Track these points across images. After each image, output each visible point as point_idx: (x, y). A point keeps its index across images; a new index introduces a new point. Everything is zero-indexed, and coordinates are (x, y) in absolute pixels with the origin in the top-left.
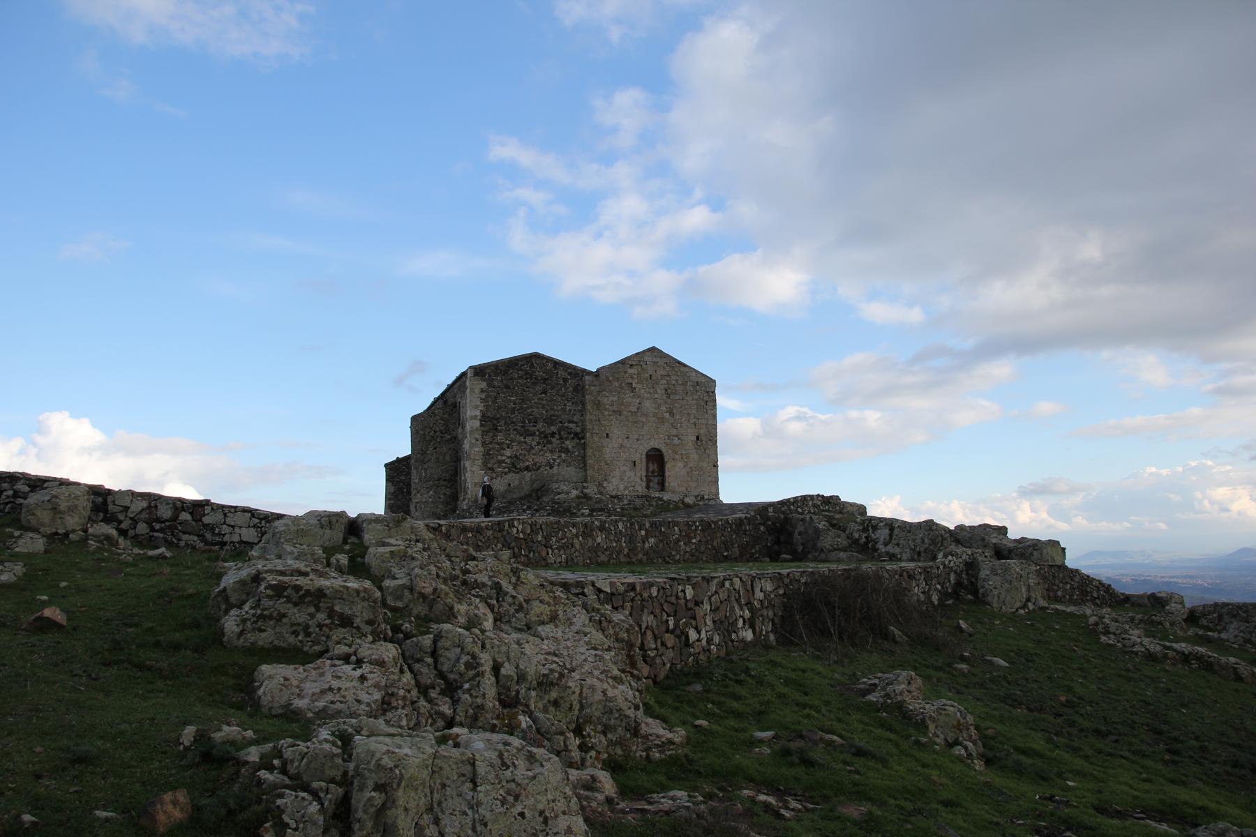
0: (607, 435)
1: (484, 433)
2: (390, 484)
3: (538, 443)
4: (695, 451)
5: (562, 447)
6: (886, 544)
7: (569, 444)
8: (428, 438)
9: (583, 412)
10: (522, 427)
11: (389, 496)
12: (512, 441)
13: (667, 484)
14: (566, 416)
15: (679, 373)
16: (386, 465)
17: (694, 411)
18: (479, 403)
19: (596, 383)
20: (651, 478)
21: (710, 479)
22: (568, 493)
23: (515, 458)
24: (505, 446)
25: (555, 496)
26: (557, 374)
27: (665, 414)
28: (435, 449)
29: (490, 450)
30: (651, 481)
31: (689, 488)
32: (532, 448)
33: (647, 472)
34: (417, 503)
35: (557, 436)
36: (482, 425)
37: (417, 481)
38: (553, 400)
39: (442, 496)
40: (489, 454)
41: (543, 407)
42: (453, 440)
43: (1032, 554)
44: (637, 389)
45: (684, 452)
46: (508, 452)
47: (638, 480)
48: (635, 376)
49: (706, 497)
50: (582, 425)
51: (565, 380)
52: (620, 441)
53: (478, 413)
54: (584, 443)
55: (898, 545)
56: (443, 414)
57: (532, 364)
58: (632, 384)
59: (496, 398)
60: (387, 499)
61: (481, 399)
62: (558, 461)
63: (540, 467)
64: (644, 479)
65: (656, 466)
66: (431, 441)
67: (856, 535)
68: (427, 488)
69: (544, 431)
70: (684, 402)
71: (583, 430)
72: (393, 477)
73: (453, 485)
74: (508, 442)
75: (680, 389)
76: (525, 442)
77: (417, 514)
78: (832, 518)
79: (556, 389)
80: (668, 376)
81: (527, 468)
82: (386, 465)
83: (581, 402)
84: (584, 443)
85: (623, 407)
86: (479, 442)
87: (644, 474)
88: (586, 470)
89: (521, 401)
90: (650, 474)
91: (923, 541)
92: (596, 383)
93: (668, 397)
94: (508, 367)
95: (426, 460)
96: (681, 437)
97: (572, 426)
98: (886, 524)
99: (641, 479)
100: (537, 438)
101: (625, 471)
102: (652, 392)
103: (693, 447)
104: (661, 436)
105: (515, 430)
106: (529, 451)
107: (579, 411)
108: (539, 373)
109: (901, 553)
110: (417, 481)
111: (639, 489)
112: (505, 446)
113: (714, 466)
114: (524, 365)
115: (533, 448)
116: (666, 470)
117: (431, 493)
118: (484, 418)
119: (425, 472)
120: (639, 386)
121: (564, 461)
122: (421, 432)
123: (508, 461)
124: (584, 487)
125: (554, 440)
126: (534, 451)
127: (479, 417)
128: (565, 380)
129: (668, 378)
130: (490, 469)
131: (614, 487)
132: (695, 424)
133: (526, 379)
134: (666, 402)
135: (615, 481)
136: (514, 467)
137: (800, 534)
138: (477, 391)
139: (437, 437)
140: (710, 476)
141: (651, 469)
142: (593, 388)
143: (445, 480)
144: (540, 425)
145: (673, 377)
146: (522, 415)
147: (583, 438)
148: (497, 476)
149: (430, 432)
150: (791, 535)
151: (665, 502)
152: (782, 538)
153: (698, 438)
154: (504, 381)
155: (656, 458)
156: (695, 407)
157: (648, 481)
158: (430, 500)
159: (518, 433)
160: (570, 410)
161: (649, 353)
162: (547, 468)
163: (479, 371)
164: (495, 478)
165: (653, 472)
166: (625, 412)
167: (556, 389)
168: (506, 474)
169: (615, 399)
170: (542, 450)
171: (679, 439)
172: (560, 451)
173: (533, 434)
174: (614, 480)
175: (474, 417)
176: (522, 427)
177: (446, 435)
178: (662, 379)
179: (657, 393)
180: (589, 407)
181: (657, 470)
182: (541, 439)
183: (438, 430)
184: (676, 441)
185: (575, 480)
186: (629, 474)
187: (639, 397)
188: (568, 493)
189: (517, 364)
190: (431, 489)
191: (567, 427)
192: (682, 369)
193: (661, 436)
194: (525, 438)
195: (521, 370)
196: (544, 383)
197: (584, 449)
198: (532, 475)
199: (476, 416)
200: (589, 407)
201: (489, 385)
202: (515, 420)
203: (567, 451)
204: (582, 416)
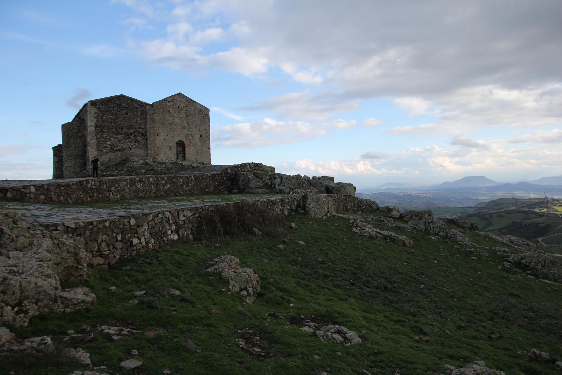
0: (158, 134)
1: (97, 134)
2: (55, 157)
3: (124, 138)
4: (199, 142)
5: (136, 140)
6: (279, 185)
7: (139, 138)
8: (70, 135)
9: (146, 123)
10: (116, 130)
11: (55, 163)
12: (111, 137)
13: (186, 157)
14: (138, 125)
15: (192, 105)
16: (53, 148)
18: (94, 119)
19: (152, 110)
20: (179, 154)
21: (207, 155)
22: (138, 162)
23: (113, 145)
24: (107, 140)
25: (132, 163)
26: (133, 105)
27: (185, 125)
28: (74, 141)
29: (100, 142)
30: (179, 156)
32: (121, 140)
33: (177, 151)
34: (66, 167)
35: (133, 135)
36: (95, 130)
37: (65, 156)
38: (131, 118)
39: (78, 164)
40: (99, 144)
41: (126, 121)
42: (83, 136)
43: (341, 190)
44: (172, 113)
45: (195, 142)
46: (109, 143)
47: (172, 155)
48: (171, 107)
49: (205, 163)
50: (146, 129)
51: (137, 108)
52: (164, 137)
53: (93, 124)
54: (147, 138)
55: (284, 186)
56: (77, 124)
57: (120, 100)
58: (169, 110)
59: (102, 116)
60: (54, 164)
61: (95, 117)
62: (134, 146)
63: (125, 150)
64: (176, 155)
65: (181, 148)
66: (71, 137)
67: (267, 181)
68: (71, 160)
69: (126, 133)
70: (195, 119)
71: (146, 132)
72: (57, 154)
73: (84, 158)
74: (109, 138)
75: (192, 113)
76: (118, 138)
77: (66, 172)
78: (257, 173)
79: (132, 112)
80: (187, 106)
81: (119, 150)
82: (53, 148)
83: (145, 119)
84: (147, 138)
85: (165, 121)
86: (94, 138)
87: (175, 153)
88: (147, 151)
89: (115, 118)
90: (178, 152)
91: (295, 184)
92: (152, 110)
93: (187, 117)
94: (108, 101)
95: (69, 146)
96: (193, 135)
97: (141, 130)
98: (280, 177)
99: (174, 155)
100: (123, 136)
101: (166, 151)
102: (179, 114)
104: (184, 135)
105: (112, 132)
106: (119, 142)
107: (144, 123)
108: (124, 105)
109: (285, 189)
110: (65, 156)
111: (173, 159)
112: (107, 140)
113: (209, 149)
114: (116, 101)
115: (121, 140)
116: (186, 151)
117: (73, 162)
118: (96, 126)
119: (69, 152)
120: (173, 111)
121: (137, 147)
122: (67, 133)
123: (109, 147)
124: (146, 159)
125: (131, 137)
126: (122, 142)
127: (94, 126)
128: (137, 108)
129: (187, 108)
130: (101, 151)
132: (199, 129)
133: (117, 107)
134: (186, 119)
135: (162, 156)
136: (112, 149)
137: (242, 181)
138: (93, 113)
139: (75, 135)
140: (206, 153)
141: (179, 150)
142: (150, 112)
143: (79, 156)
144: (125, 130)
145: (189, 107)
146: (116, 125)
147: (146, 136)
148: (104, 154)
149: (71, 133)
150: (238, 181)
151: (184, 166)
152: (234, 183)
153: (201, 136)
154: (107, 108)
155: (181, 145)
157: (178, 156)
158: (73, 165)
159: (114, 133)
160: (139, 122)
162: (129, 150)
163: (93, 103)
164: (103, 155)
165: (180, 151)
166: (166, 124)
167: (132, 112)
168: (108, 153)
169: (161, 117)
170: (126, 141)
171: (192, 136)
172: (135, 142)
173: (121, 134)
174: (161, 155)
175: (92, 126)
176: (116, 130)
177: (79, 134)
178: (184, 108)
179: (181, 115)
180: (148, 121)
181: (181, 151)
182: (125, 136)
183: (75, 131)
184: (190, 137)
185: (142, 155)
186: (169, 152)
187: (173, 116)
188: (138, 162)
189: (113, 100)
190: (72, 160)
191: (138, 131)
192: (194, 103)
193: (184, 135)
194: (117, 136)
195: (115, 103)
196: (126, 109)
197: (147, 141)
198: (121, 153)
199: (93, 125)
200: (149, 121)
201: (99, 110)
202: (112, 127)
203: (138, 142)
204: (145, 125)
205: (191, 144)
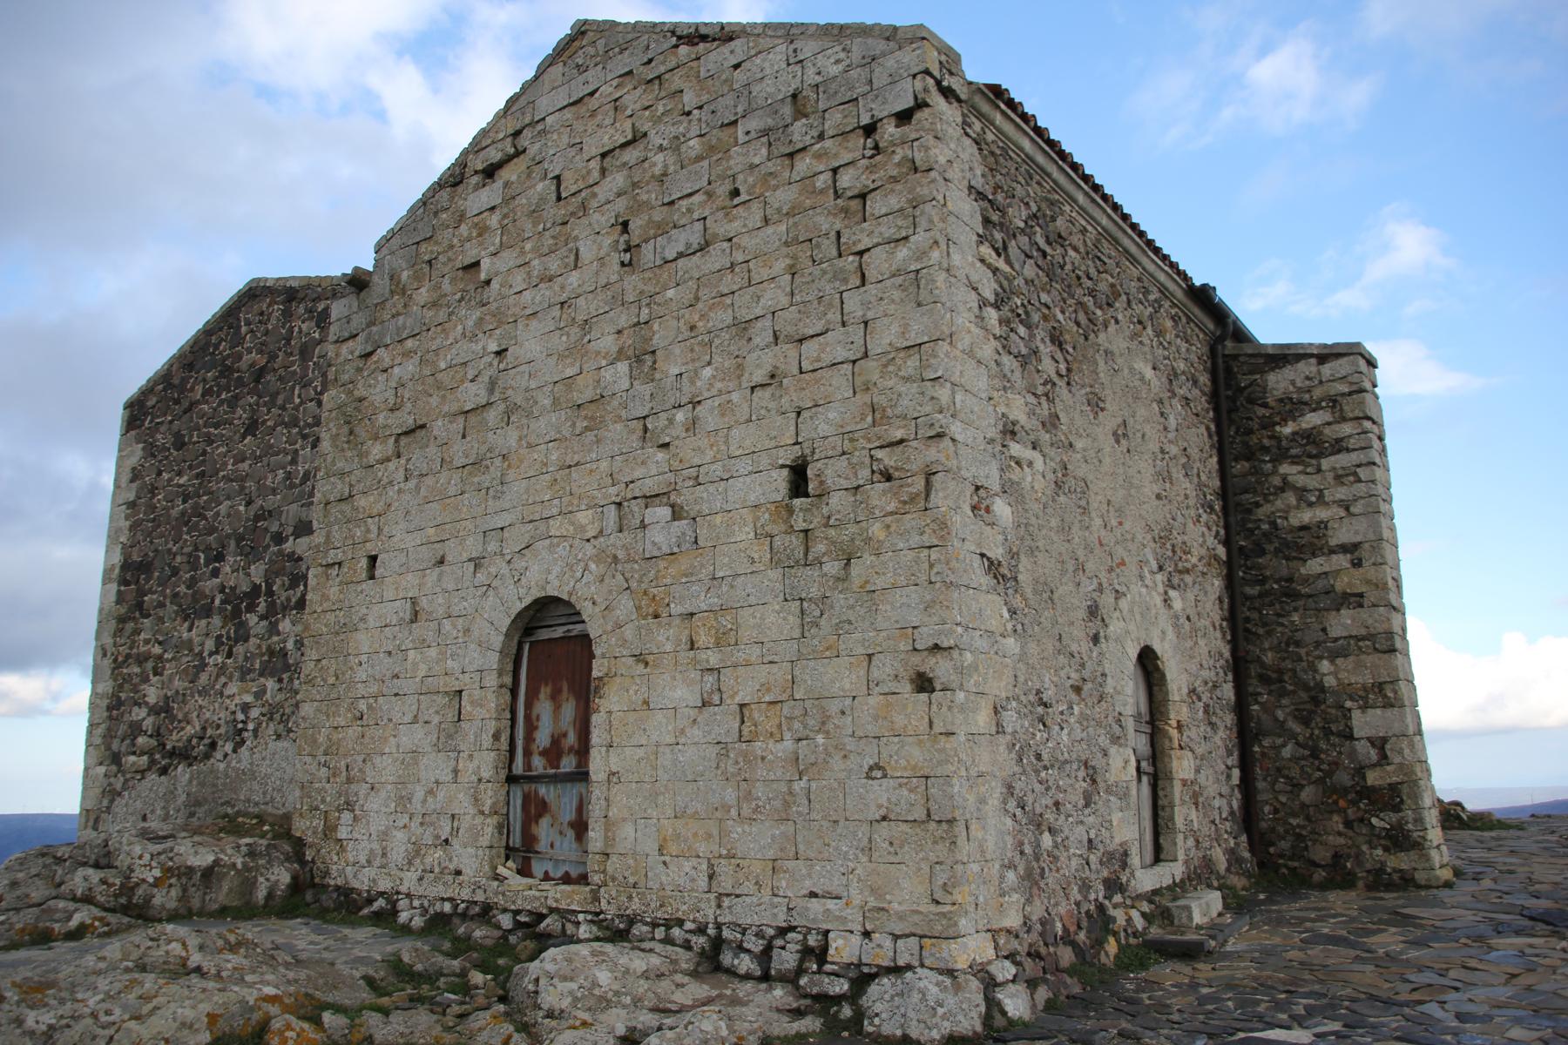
17: (774, 296)
21: (881, 793)
27: (607, 374)
31: (724, 868)
35: (262, 606)
47: (463, 805)
49: (844, 948)
70: (716, 258)
103: (761, 552)
131: (376, 846)
140: (876, 770)
141: (543, 738)
156: (780, 265)
161: (558, 69)
184: (661, 531)
186: (435, 767)
193: (584, 517)
205: (666, 638)
